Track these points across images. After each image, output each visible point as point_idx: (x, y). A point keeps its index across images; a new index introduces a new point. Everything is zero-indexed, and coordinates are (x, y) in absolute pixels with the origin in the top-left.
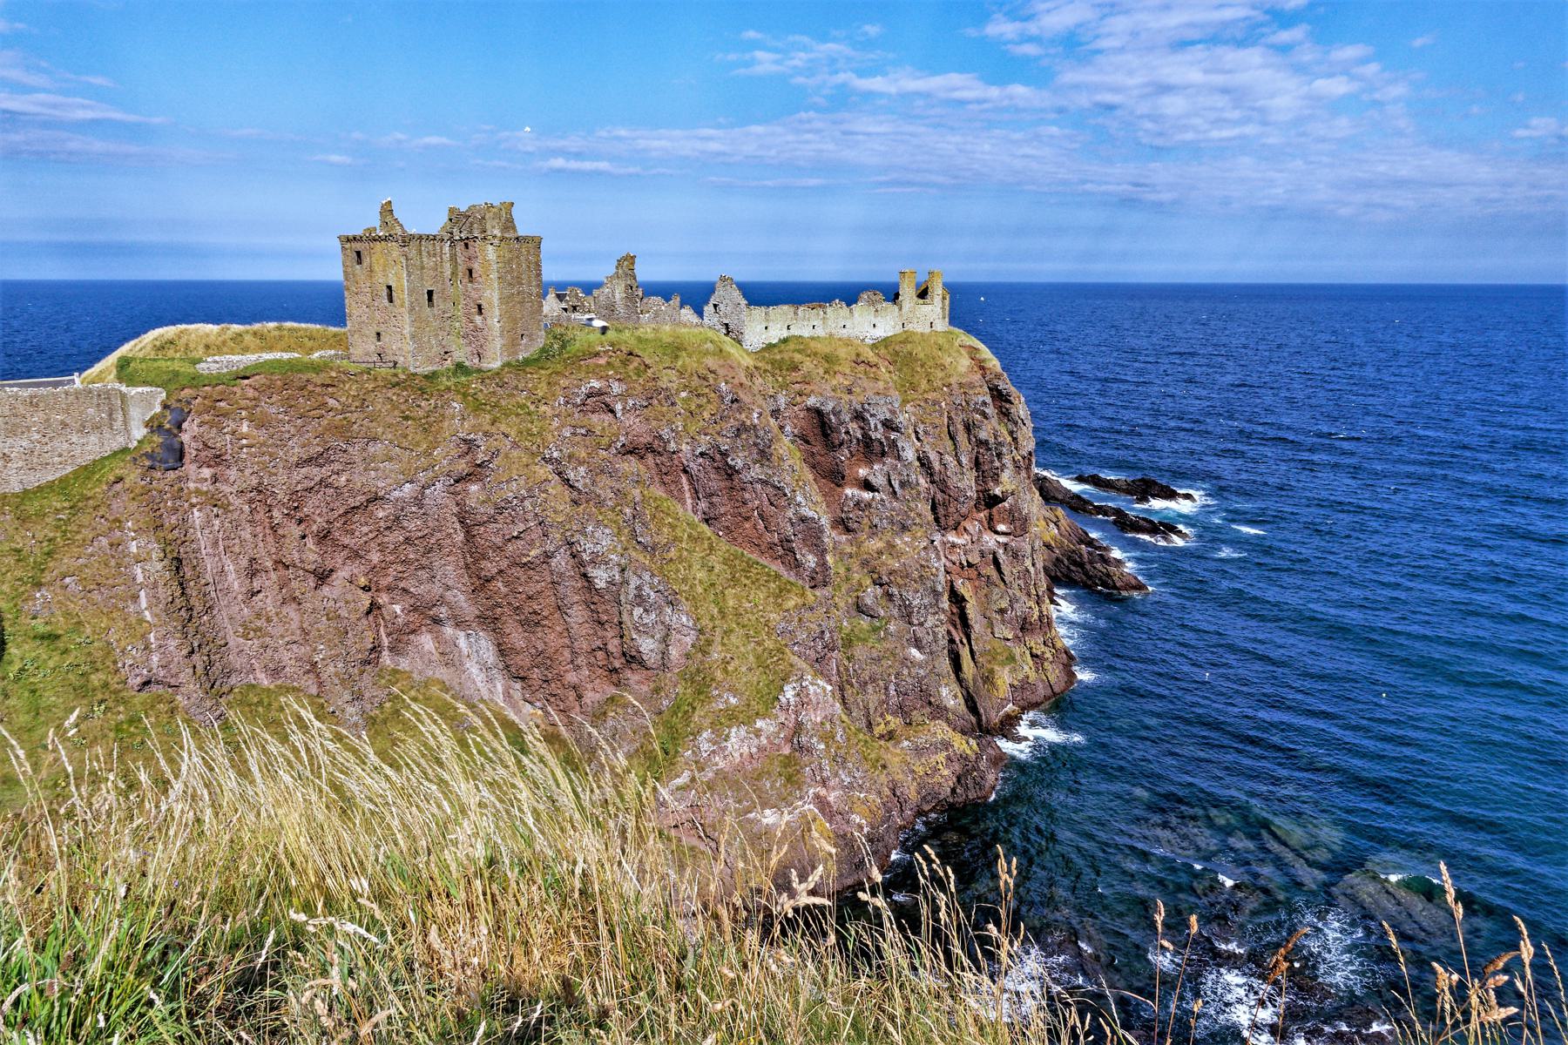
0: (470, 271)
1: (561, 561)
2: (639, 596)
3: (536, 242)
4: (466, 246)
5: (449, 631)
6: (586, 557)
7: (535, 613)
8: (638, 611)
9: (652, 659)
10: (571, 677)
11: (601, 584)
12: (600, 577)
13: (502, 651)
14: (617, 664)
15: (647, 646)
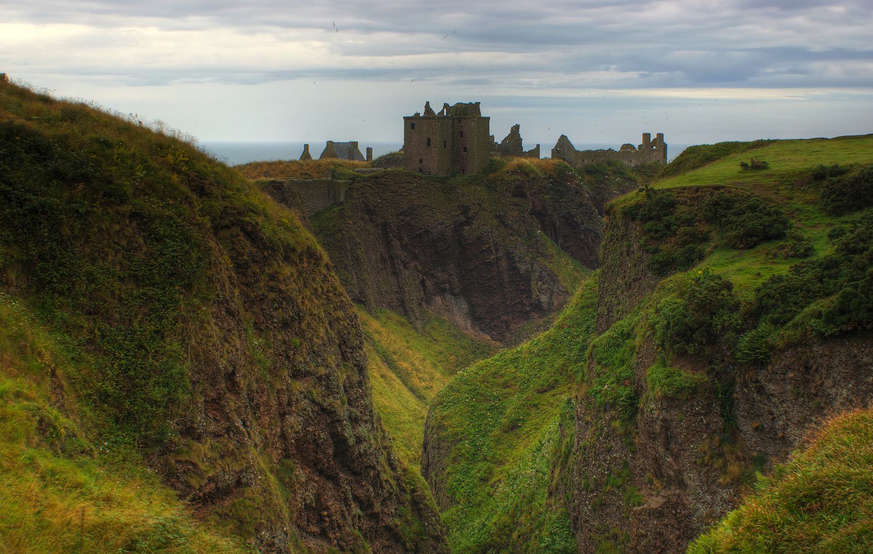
0: (461, 133)
1: (504, 263)
2: (540, 277)
3: (488, 119)
4: (460, 121)
5: (448, 296)
6: (516, 259)
7: (490, 286)
8: (540, 283)
9: (545, 306)
10: (505, 318)
11: (522, 272)
12: (523, 268)
13: (472, 306)
14: (528, 309)
15: (544, 299)
